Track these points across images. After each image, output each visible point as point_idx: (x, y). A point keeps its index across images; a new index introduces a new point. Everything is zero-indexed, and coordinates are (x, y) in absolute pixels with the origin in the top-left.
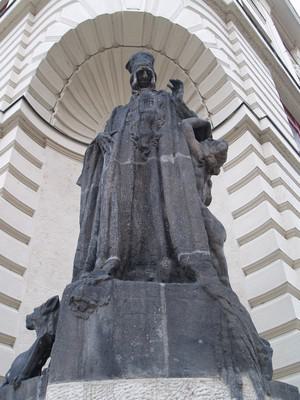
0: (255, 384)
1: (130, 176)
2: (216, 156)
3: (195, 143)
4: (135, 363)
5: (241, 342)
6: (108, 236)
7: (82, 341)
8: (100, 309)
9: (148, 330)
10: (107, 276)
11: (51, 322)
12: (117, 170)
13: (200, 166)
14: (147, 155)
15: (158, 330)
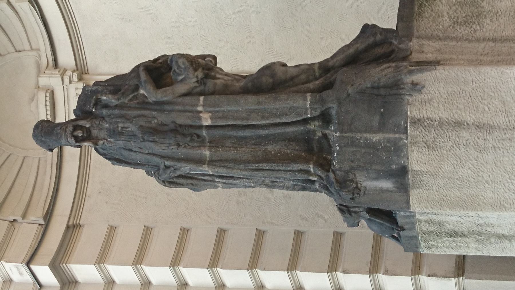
0: (411, 72)
1: (221, 153)
2: (196, 70)
4: (399, 157)
7: (383, 191)
8: (358, 179)
9: (374, 147)
10: (331, 175)
11: (357, 209)
12: (217, 164)
13: (205, 84)
14: (198, 136)
15: (374, 140)
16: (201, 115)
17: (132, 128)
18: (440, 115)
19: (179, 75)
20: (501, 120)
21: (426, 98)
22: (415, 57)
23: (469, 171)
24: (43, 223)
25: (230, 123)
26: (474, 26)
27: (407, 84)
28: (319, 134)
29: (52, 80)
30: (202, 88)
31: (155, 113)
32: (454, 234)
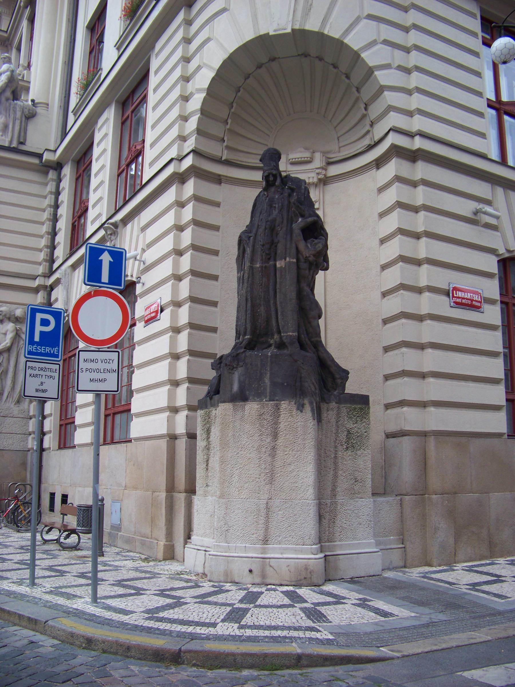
0: (311, 403)
2: (314, 255)
3: (302, 245)
5: (306, 384)
6: (246, 322)
7: (232, 385)
10: (243, 350)
13: (305, 262)
14: (269, 259)
16: (283, 260)
17: (275, 213)
18: (282, 423)
19: (311, 245)
20: (278, 463)
21: (294, 413)
22: (324, 406)
23: (245, 442)
24: (223, 159)
25: (278, 280)
26: (346, 444)
27: (303, 400)
28: (272, 342)
29: (318, 161)
30: (302, 260)
31: (284, 229)
32: (208, 432)
